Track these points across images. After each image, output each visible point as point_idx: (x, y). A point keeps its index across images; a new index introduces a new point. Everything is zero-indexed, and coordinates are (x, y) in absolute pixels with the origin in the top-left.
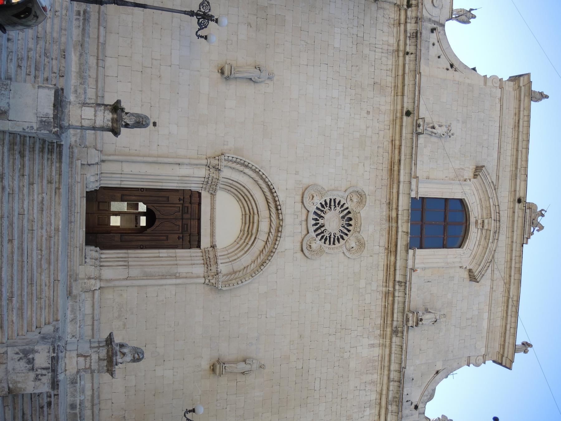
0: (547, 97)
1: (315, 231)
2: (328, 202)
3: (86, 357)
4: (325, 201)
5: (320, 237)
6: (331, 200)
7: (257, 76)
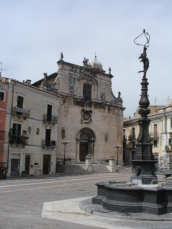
7: (63, 131)
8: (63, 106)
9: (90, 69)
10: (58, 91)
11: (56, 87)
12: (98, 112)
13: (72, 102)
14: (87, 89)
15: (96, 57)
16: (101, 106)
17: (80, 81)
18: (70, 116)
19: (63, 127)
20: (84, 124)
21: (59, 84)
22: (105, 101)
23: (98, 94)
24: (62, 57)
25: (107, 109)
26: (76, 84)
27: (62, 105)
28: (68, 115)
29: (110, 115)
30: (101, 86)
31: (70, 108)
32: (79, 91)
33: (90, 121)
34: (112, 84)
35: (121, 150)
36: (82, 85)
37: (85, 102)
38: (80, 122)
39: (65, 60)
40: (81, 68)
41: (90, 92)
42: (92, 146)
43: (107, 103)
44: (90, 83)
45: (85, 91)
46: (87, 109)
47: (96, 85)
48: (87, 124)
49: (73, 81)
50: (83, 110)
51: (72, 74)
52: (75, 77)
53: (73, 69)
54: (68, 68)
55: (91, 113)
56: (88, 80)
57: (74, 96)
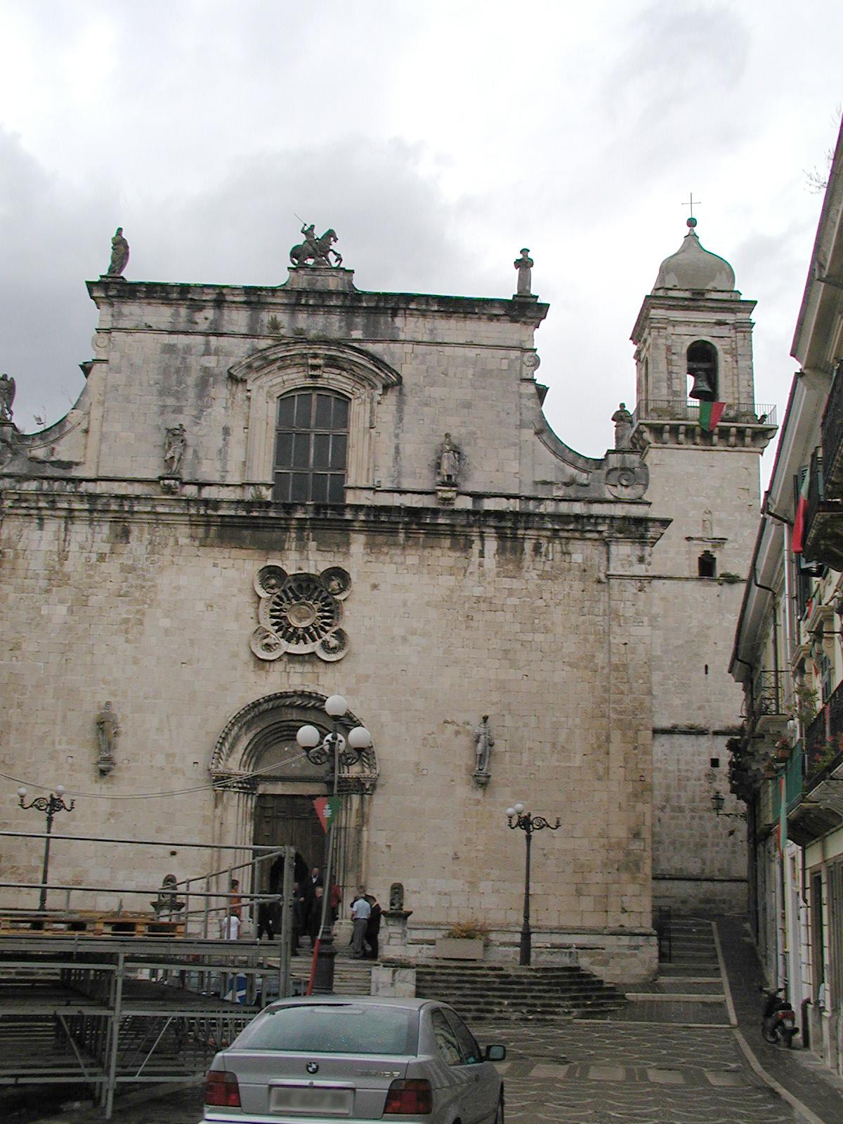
0: (120, 230)
1: (314, 640)
2: (275, 620)
3: (390, 937)
4: (273, 625)
5: (322, 633)
6: (273, 617)
8: (111, 567)
9: (330, 294)
10: (76, 473)
11: (63, 452)
12: (408, 578)
13: (183, 532)
14: (310, 431)
15: (692, 223)
16: (434, 532)
17: (244, 381)
18: (165, 623)
19: (103, 698)
20: (279, 667)
21: (86, 431)
22: (469, 487)
23: (408, 449)
24: (120, 248)
25: (491, 545)
26: (217, 412)
27: (102, 557)
28: (146, 620)
29: (516, 584)
30: (437, 392)
31: (161, 569)
32: (236, 454)
33: (334, 642)
34: (537, 363)
35: (636, 846)
36: (266, 411)
37: (300, 516)
38: (245, 656)
39: (131, 274)
40: (254, 298)
41: (341, 443)
42: (353, 821)
43: (489, 505)
44: (335, 380)
45: (288, 441)
46: (316, 562)
47: (386, 388)
48: (308, 668)
49: (192, 393)
50: (271, 574)
51: (188, 350)
52: (210, 362)
53: (199, 317)
54: (160, 315)
55: (342, 590)
56: (315, 367)
57: (201, 485)
